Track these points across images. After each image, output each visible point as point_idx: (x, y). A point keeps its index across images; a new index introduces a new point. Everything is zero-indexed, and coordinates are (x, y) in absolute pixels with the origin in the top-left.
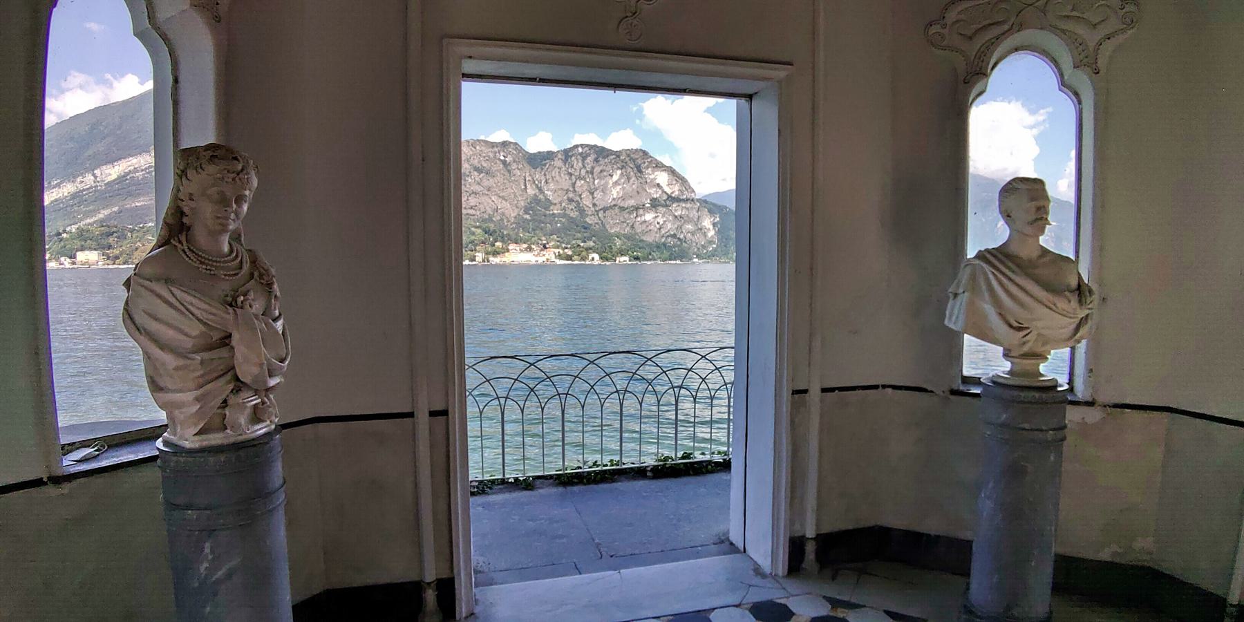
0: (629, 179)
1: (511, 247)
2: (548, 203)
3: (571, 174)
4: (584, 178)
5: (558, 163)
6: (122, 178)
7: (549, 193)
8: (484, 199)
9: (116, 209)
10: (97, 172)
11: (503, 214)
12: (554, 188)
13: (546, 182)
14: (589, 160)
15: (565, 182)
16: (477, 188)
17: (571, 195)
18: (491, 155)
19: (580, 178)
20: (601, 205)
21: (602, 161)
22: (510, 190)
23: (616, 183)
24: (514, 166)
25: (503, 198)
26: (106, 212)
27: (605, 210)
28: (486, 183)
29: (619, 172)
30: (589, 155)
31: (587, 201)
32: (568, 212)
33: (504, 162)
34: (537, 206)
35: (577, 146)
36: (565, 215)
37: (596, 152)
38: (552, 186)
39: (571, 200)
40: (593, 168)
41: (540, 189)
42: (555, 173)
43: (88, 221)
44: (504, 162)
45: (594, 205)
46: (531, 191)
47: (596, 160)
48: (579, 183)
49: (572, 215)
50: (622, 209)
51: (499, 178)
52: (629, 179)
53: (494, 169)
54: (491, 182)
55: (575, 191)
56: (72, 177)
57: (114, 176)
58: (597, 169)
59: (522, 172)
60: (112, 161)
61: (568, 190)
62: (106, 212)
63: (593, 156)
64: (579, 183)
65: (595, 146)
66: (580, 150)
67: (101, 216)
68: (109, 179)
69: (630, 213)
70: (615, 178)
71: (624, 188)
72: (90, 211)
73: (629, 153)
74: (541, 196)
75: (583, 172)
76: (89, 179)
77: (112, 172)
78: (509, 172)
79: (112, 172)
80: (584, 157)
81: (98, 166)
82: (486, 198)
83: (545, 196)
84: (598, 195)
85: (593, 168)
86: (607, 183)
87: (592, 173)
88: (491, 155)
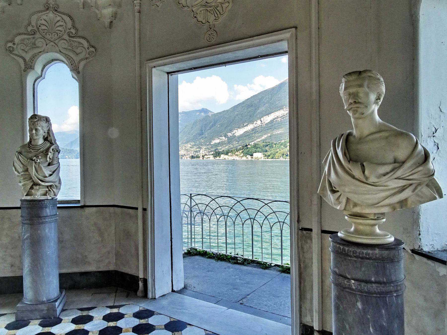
6: (272, 121)
10: (262, 119)
56: (252, 122)
57: (269, 121)
68: (267, 122)
72: (259, 136)
76: (259, 122)
79: (267, 119)
81: (262, 117)
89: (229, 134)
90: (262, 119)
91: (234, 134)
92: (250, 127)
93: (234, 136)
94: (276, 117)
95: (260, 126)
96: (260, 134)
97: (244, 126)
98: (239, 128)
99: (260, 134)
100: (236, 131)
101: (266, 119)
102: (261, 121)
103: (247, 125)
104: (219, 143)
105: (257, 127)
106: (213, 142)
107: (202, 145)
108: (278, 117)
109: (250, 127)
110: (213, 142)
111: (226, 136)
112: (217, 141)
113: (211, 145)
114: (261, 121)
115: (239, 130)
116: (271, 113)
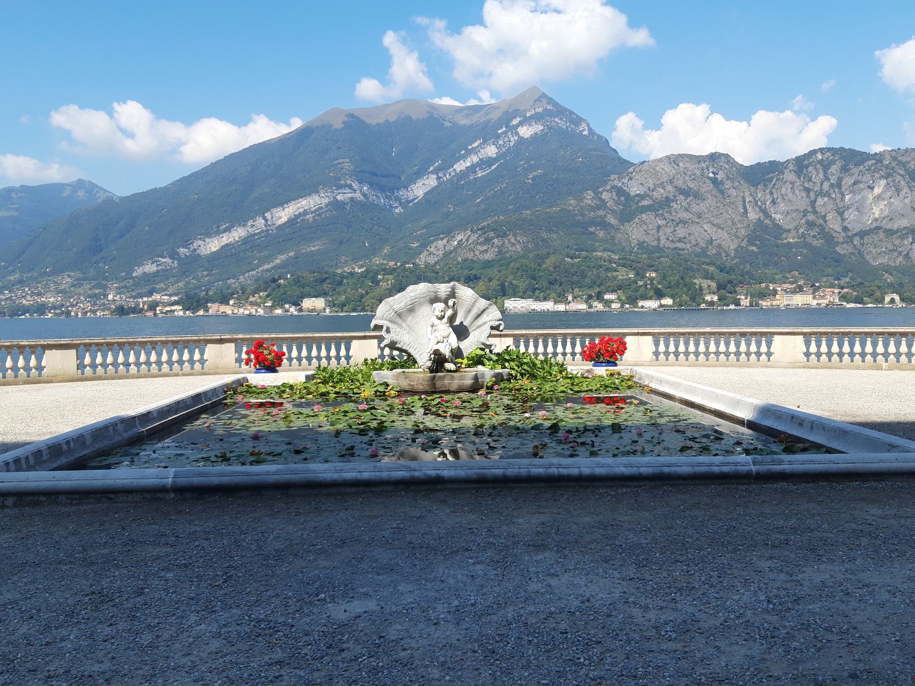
0: (898, 190)
1: (738, 289)
2: (778, 230)
3: (808, 190)
4: (827, 194)
5: (789, 176)
6: (292, 221)
7: (778, 217)
8: (694, 229)
9: (292, 254)
10: (268, 215)
11: (720, 246)
12: (786, 208)
13: (774, 202)
14: (834, 169)
15: (801, 201)
16: (685, 215)
17: (811, 217)
18: (698, 173)
19: (821, 194)
20: (855, 228)
21: (855, 170)
22: (725, 215)
23: (879, 198)
24: (728, 184)
25: (718, 226)
26: (283, 257)
27: (862, 234)
28: (695, 208)
29: (883, 182)
30: (833, 162)
31: (834, 224)
32: (809, 240)
33: (714, 181)
34: (765, 234)
35: (814, 152)
36: (806, 245)
37: (843, 158)
38: (782, 207)
39: (811, 225)
40: (840, 179)
41: (765, 212)
42: (786, 190)
43: (266, 267)
44: (714, 181)
45: (845, 229)
46: (753, 215)
47: (845, 169)
48: (820, 201)
49: (815, 243)
50: (890, 233)
51: (711, 201)
52: (898, 190)
53: (703, 190)
54: (702, 207)
55: (815, 212)
56: (242, 222)
57: (284, 219)
58: (848, 181)
59: (740, 192)
60: (282, 203)
61: (805, 213)
62: (283, 257)
63: (839, 164)
64: (820, 201)
65: (842, 149)
66: (820, 157)
67: (278, 261)
69: (902, 238)
70: (877, 191)
71: (890, 204)
73: (896, 155)
74: (767, 221)
75: (826, 186)
76: (260, 222)
77: (283, 215)
78: (722, 192)
79: (283, 215)
80: (826, 166)
81: (268, 210)
82: (698, 229)
83: (773, 220)
84: (851, 215)
85: (840, 179)
86: (864, 198)
87: (839, 186)
88: (698, 173)
89: (182, 250)
90: (268, 215)
91: (195, 250)
92: (237, 234)
93: (195, 257)
94: (301, 210)
95: (262, 231)
96: (266, 253)
97: (218, 233)
98: (209, 235)
99: (266, 253)
100: (200, 242)
101: (277, 215)
102: (266, 221)
103: (228, 230)
104: (156, 274)
105: (255, 234)
106: (138, 272)
107: (106, 279)
108: (305, 213)
109: (237, 234)
110: (138, 272)
111: (173, 255)
112: (150, 268)
113: (133, 278)
114: (266, 221)
115: (207, 240)
116: (290, 201)
